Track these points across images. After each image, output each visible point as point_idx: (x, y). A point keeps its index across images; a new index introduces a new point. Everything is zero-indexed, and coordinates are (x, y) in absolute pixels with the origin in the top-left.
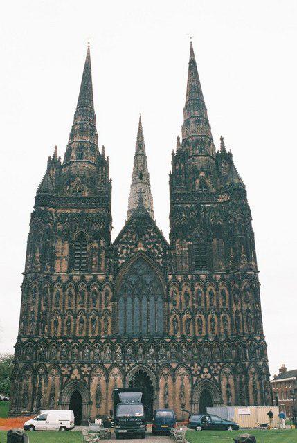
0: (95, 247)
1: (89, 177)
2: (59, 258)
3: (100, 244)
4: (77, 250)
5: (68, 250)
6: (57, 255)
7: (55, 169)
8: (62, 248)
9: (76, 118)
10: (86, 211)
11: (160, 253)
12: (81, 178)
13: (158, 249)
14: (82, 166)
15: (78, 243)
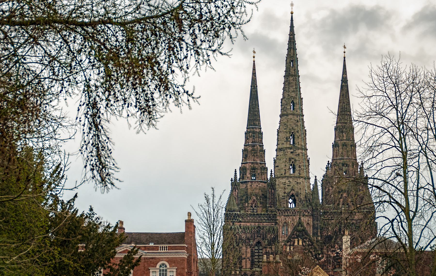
0: (269, 251)
1: (261, 194)
2: (244, 258)
3: (272, 249)
4: (256, 253)
5: (250, 253)
6: (243, 256)
7: (237, 191)
8: (246, 252)
9: (247, 138)
10: (261, 225)
11: (312, 256)
12: (256, 196)
13: (311, 252)
14: (255, 185)
15: (256, 248)
